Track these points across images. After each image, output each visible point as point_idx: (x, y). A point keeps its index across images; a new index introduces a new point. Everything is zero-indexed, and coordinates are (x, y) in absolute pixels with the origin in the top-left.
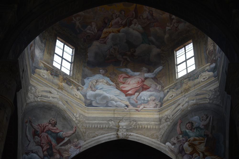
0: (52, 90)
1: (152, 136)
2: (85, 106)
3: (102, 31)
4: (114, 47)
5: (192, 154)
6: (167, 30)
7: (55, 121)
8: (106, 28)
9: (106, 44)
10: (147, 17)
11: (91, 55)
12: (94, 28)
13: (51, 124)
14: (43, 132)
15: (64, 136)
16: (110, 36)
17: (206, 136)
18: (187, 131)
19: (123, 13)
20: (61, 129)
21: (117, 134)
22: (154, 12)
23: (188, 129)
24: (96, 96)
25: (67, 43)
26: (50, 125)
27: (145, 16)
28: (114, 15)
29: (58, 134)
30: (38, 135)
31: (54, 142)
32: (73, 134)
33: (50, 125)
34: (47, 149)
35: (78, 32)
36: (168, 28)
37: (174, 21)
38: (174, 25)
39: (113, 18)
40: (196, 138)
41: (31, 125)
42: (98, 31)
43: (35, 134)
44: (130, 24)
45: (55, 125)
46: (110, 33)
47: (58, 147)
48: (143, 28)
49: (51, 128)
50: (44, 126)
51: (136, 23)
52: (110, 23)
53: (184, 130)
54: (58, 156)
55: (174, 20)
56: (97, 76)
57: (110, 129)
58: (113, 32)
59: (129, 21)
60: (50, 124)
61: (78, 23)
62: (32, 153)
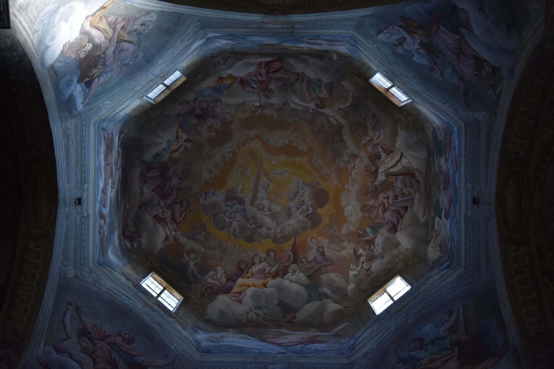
0: (133, 298)
2: (196, 349)
3: (235, 281)
4: (257, 311)
6: (350, 277)
8: (243, 278)
9: (242, 304)
10: (315, 259)
12: (221, 276)
13: (122, 337)
16: (249, 291)
18: (413, 353)
19: (272, 254)
22: (325, 249)
23: (413, 351)
25: (170, 287)
26: (120, 338)
28: (257, 258)
30: (91, 340)
32: (166, 365)
33: (120, 338)
35: (192, 280)
36: (352, 273)
37: (362, 259)
38: (362, 267)
39: (255, 262)
40: (433, 357)
42: (227, 280)
43: (83, 332)
45: (130, 341)
46: (249, 286)
48: (308, 276)
49: (121, 343)
50: (106, 334)
51: (295, 271)
52: (250, 271)
53: (405, 355)
55: (362, 257)
58: (254, 286)
59: (284, 268)
60: (120, 336)
61: (192, 265)
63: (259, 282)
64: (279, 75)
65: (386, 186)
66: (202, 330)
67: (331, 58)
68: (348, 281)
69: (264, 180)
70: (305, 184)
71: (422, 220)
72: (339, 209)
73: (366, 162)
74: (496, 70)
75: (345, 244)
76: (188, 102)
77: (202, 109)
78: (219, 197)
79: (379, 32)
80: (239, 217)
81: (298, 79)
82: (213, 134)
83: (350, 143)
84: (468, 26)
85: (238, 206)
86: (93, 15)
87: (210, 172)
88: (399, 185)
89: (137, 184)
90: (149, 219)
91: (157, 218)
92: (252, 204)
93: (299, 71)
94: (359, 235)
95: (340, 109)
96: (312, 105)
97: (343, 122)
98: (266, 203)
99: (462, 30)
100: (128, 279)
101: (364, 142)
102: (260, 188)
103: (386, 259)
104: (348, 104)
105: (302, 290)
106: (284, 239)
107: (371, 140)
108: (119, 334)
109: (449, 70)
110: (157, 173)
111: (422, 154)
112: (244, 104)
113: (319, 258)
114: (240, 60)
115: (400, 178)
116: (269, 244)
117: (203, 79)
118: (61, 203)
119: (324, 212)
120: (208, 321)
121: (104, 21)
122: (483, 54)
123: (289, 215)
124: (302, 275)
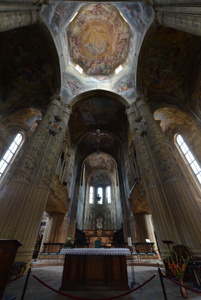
1: (109, 88)
5: (122, 91)
11: (88, 72)
16: (94, 67)
17: (127, 83)
20: (78, 85)
24: (90, 81)
27: (105, 59)
31: (75, 88)
34: (73, 89)
36: (113, 63)
42: (91, 65)
43: (68, 83)
44: (101, 63)
45: (76, 83)
47: (77, 89)
48: (105, 64)
54: (77, 92)
56: (91, 77)
61: (84, 61)
63: (96, 65)
64: (99, 9)
65: (121, 42)
66: (87, 77)
67: (111, 5)
68: (112, 65)
69: (96, 40)
70: (105, 41)
71: (127, 52)
72: (111, 48)
73: (117, 36)
74: (144, 25)
75: (112, 56)
76: (79, 19)
77: (82, 20)
78: (87, 45)
79: (122, 7)
80: (92, 50)
81: (103, 11)
82: (85, 28)
83: (114, 30)
84: (140, 11)
85: (92, 47)
86: (56, 8)
87: (86, 38)
88: (123, 42)
89: (71, 42)
90: (75, 51)
91: (76, 51)
92: (94, 46)
93: (104, 8)
94: (115, 54)
95: (113, 20)
96: (107, 19)
97: (113, 24)
98: (97, 46)
99: (139, 12)
100: (73, 68)
101: (117, 30)
102: (96, 42)
103: (119, 60)
104: (115, 19)
105: (104, 67)
106: (101, 55)
107: (119, 30)
108: (74, 82)
109: (135, 21)
110: (75, 39)
111: (129, 35)
112: (91, 18)
113: (107, 60)
114: (90, 5)
115: (124, 40)
116: (98, 56)
117: (82, 12)
118: (59, 58)
119: (108, 48)
120: (88, 74)
121: (59, 8)
122: (142, 20)
123: (102, 49)
124: (104, 63)
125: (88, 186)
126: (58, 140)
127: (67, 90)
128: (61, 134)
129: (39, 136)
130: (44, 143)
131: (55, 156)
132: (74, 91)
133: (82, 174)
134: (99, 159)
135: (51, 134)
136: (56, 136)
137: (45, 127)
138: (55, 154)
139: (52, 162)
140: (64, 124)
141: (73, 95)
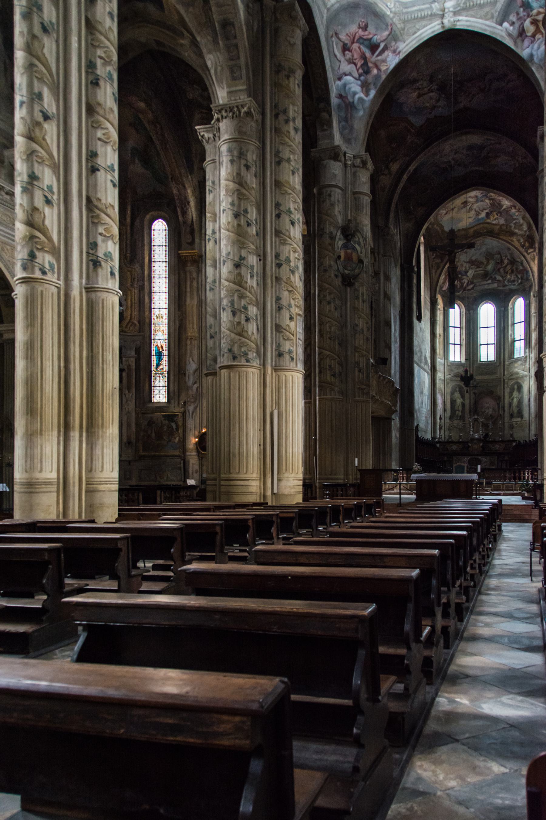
7: (365, 22)
14: (353, 43)
15: (379, 41)
21: (442, 23)
29: (372, 40)
30: (349, 50)
31: (368, 54)
34: (362, 65)
41: (338, 38)
45: (365, 28)
47: (374, 59)
54: (375, 71)
57: (433, 16)
62: (346, 75)
125: (440, 305)
126: (363, 294)
127: (347, 87)
128: (365, 275)
129: (329, 303)
130: (341, 316)
131: (365, 338)
132: (367, 71)
133: (415, 281)
134: (477, 201)
135: (346, 286)
136: (356, 284)
137: (333, 275)
138: (365, 330)
139: (364, 352)
140: (365, 239)
141: (367, 95)
